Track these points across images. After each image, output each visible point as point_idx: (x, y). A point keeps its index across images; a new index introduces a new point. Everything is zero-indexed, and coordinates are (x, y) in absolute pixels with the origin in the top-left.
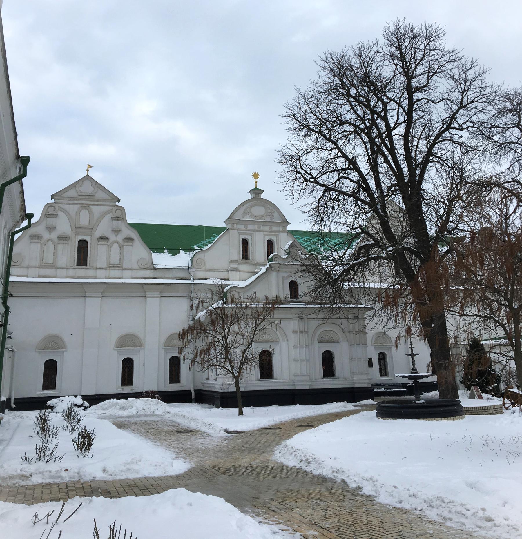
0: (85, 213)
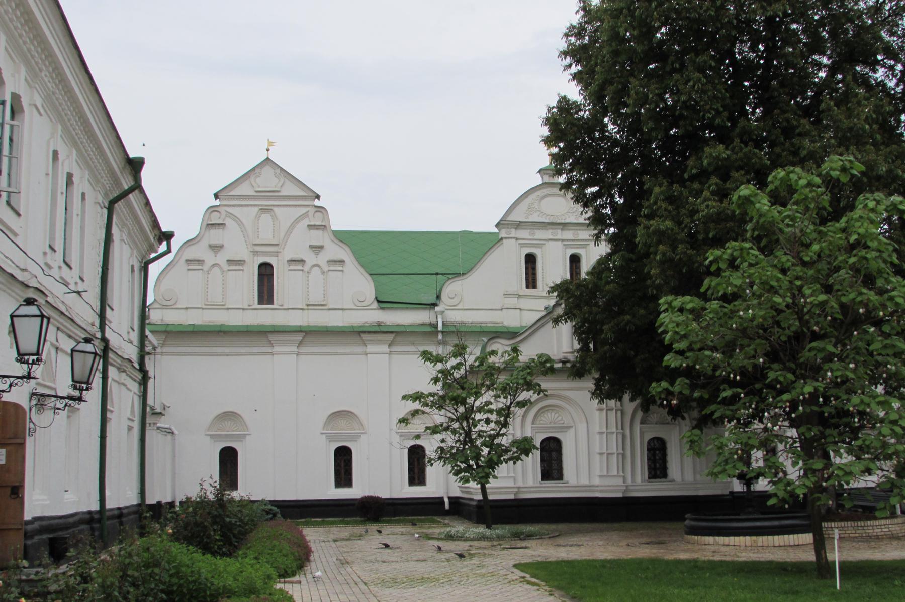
0: (266, 217)
